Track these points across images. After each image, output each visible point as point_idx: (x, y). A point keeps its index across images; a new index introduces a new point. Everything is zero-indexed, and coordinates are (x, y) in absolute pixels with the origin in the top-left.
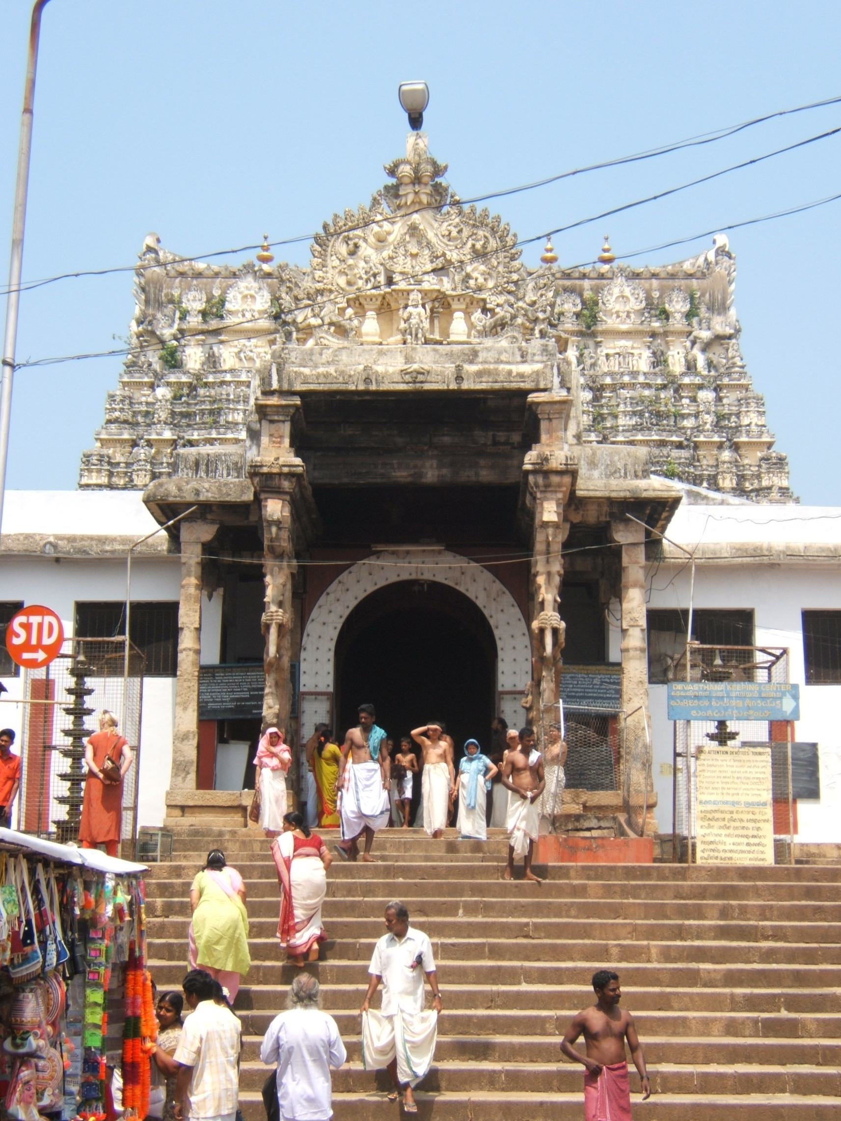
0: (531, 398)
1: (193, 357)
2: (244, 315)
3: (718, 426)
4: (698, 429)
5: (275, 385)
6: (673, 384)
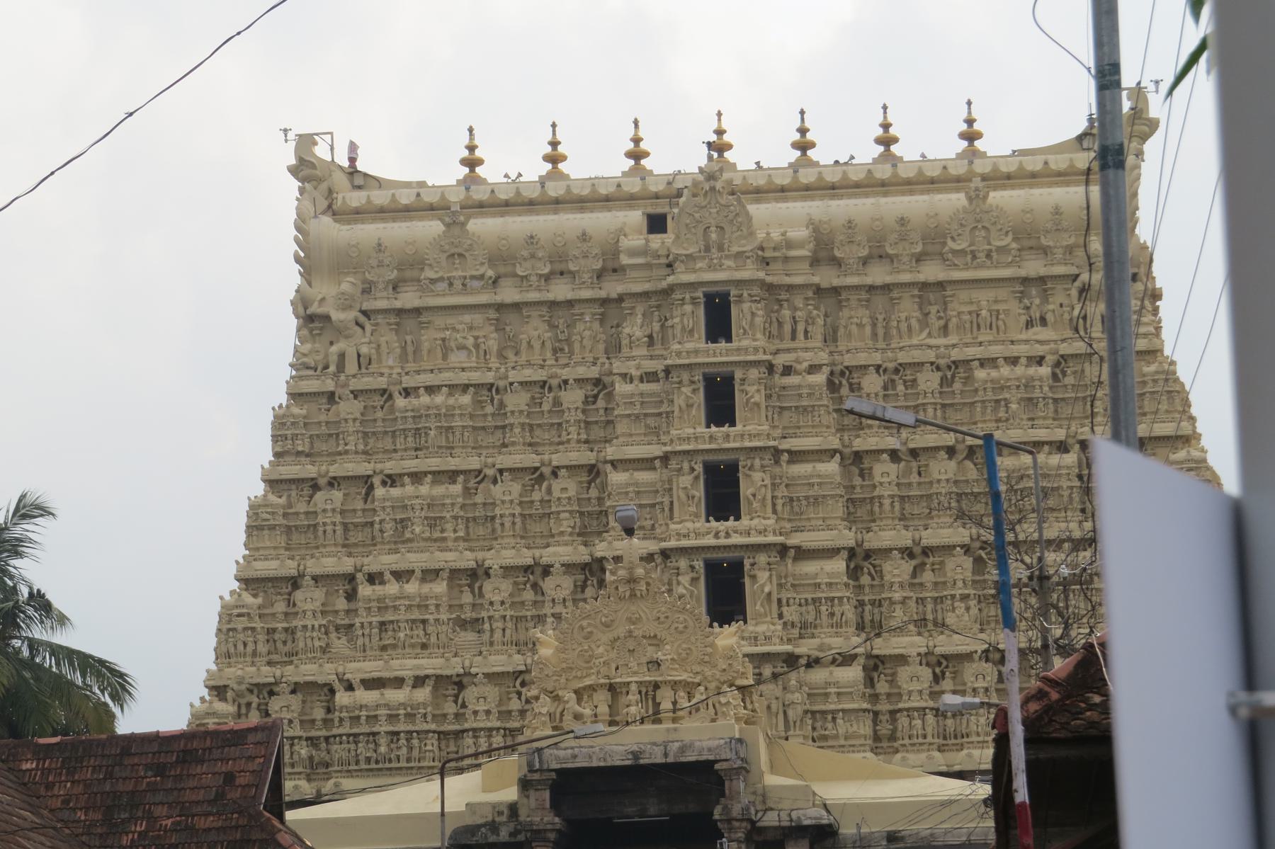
0: (717, 766)
2: (451, 284)
5: (537, 766)
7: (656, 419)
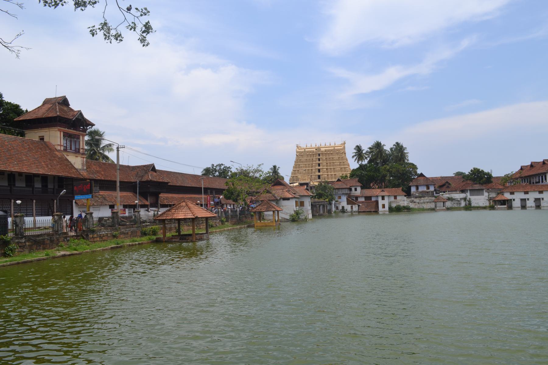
7: (316, 161)
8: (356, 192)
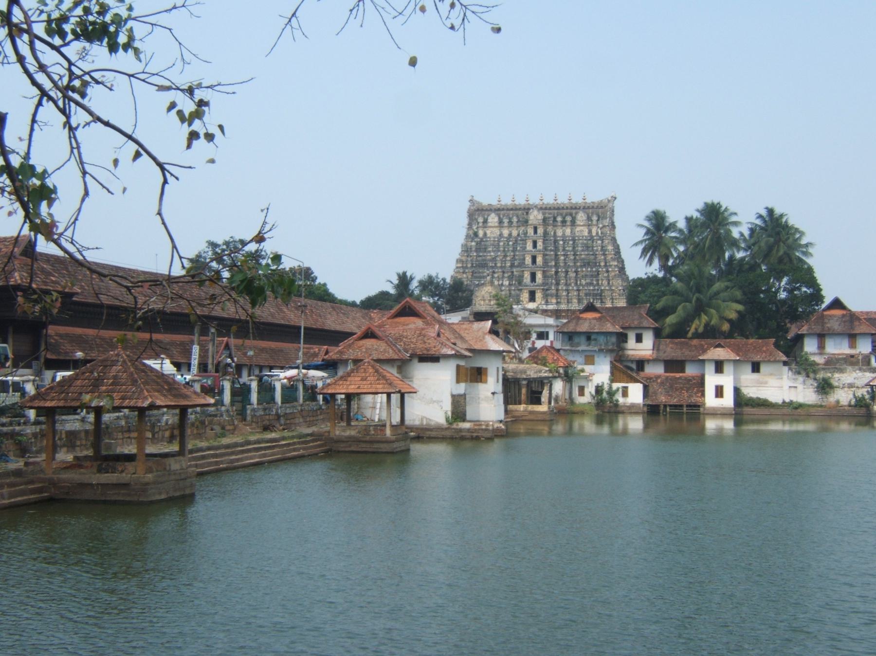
1: (481, 233)
3: (602, 250)
4: (597, 250)
6: (592, 238)
8: (639, 346)
